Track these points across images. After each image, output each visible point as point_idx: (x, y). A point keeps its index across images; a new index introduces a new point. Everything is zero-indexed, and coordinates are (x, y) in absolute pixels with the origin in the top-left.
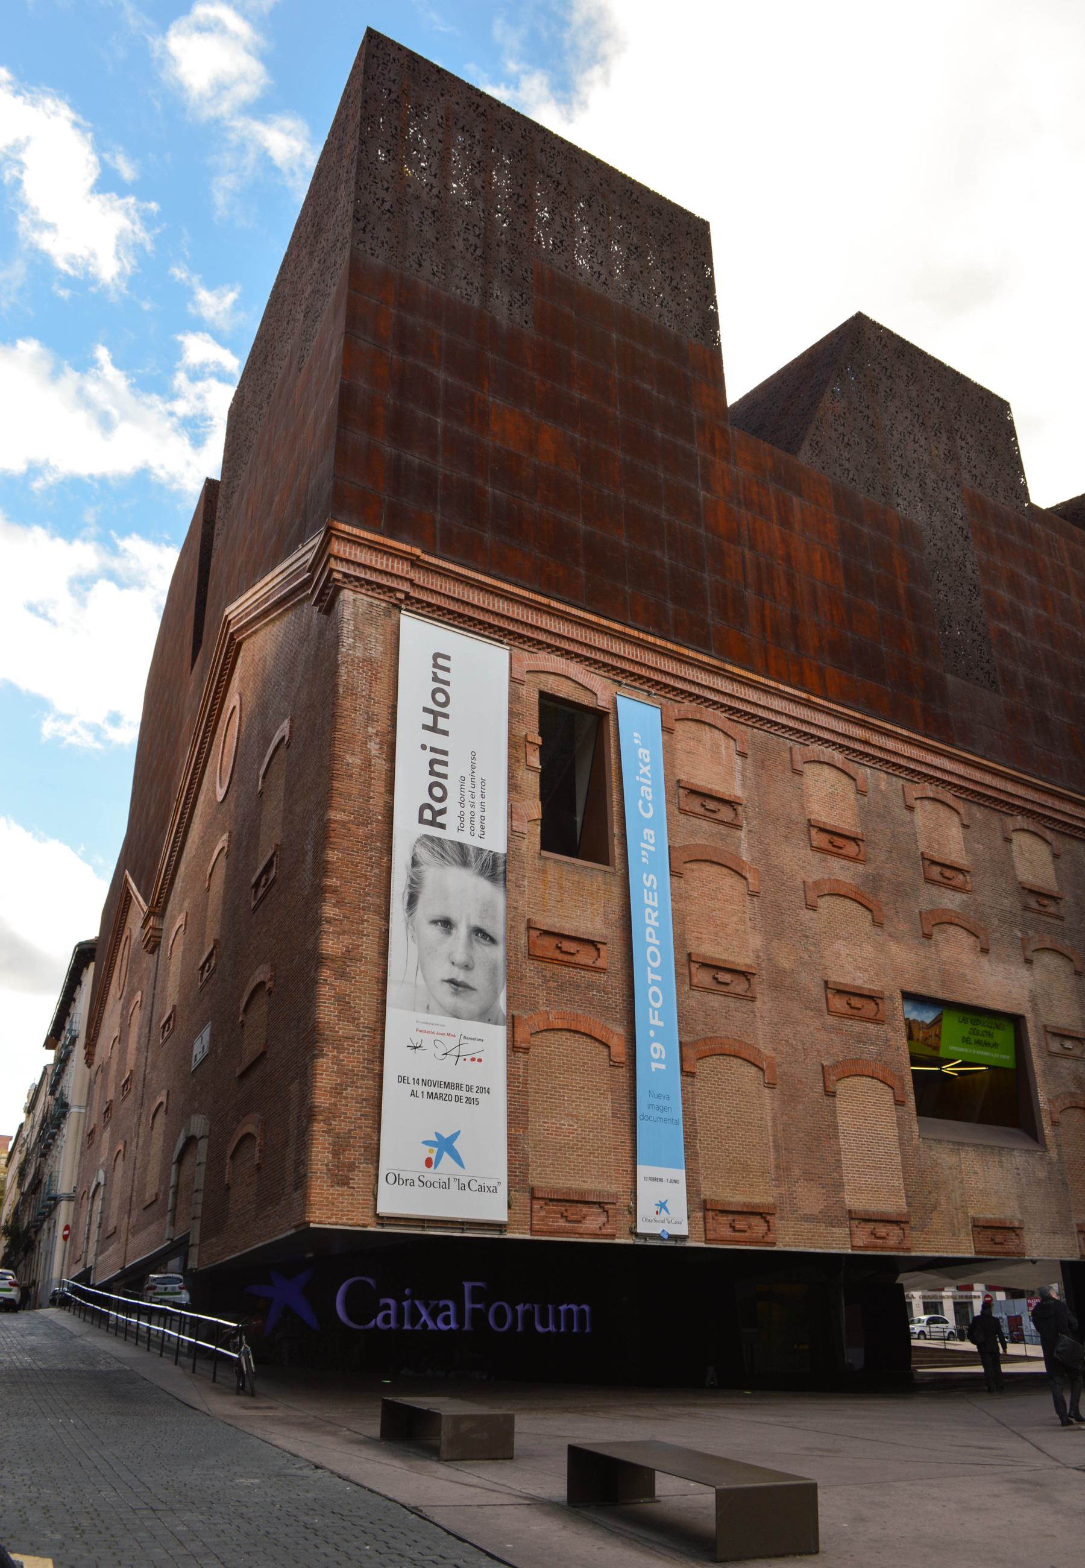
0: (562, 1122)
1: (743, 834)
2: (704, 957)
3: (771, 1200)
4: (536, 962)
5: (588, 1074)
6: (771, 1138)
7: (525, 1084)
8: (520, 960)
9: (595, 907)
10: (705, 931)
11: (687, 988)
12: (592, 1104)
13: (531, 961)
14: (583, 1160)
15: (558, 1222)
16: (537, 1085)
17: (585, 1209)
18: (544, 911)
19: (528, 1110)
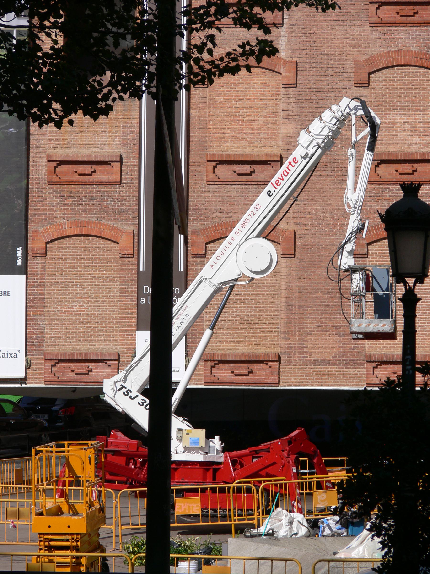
0: (74, 304)
1: (283, 31)
2: (220, 155)
3: (277, 350)
4: (55, 187)
5: (99, 266)
6: (283, 300)
7: (43, 278)
8: (40, 187)
9: (114, 131)
10: (229, 131)
11: (204, 183)
12: (102, 288)
13: (51, 186)
14: (92, 330)
15: (68, 375)
16: (53, 279)
17: (91, 365)
18: (64, 144)
19: (44, 298)
